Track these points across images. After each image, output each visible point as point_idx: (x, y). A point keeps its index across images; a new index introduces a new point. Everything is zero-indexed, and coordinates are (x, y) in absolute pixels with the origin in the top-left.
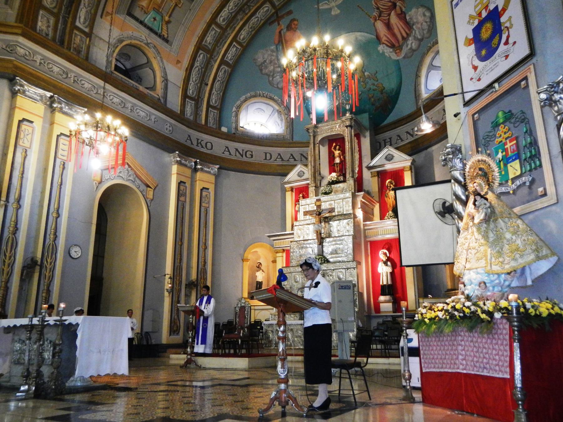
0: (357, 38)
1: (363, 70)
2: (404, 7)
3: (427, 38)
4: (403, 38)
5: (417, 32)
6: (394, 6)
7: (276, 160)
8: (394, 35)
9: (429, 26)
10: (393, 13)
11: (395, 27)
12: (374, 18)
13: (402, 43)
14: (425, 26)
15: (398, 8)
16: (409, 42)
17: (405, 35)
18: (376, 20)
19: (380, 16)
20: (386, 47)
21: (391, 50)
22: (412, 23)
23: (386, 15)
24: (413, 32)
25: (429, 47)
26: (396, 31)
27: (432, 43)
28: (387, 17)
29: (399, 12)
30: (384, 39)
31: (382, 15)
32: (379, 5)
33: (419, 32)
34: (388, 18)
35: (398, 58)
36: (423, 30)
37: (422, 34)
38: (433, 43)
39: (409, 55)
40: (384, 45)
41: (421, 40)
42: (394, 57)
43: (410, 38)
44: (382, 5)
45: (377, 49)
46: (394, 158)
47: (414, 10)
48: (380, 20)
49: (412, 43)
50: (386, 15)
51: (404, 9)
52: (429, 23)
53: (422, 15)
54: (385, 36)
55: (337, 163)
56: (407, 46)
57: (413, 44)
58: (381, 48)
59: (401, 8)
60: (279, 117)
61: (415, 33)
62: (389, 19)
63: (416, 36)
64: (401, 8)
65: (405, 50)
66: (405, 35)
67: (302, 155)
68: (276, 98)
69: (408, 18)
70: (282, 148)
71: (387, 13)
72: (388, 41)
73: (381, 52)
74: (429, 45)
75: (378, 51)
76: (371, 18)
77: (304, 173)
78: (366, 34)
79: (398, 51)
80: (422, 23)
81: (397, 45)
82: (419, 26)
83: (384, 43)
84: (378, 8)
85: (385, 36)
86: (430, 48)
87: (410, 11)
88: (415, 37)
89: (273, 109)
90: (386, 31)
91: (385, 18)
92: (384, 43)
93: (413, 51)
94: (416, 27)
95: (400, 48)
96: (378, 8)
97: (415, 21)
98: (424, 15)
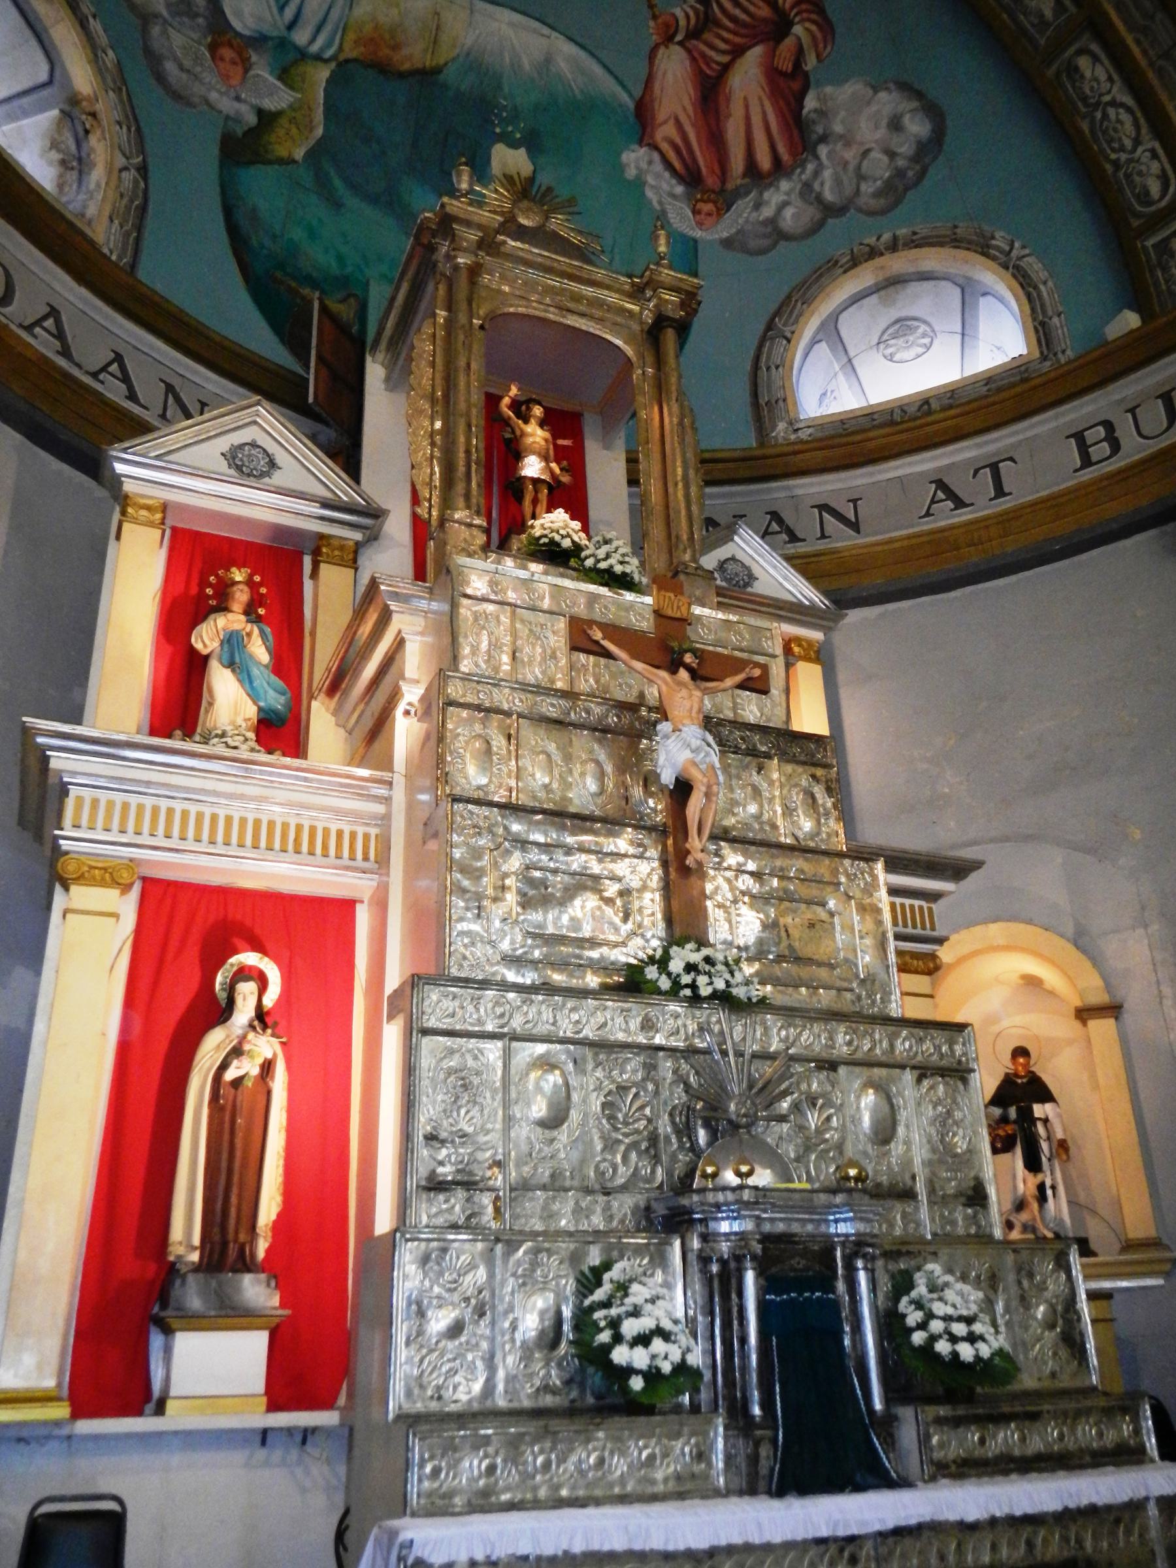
0: (548, 60)
2: (818, 56)
3: (871, 213)
4: (751, 167)
5: (827, 174)
6: (779, 28)
7: (29, 328)
8: (716, 140)
9: (900, 173)
10: (756, 53)
11: (737, 110)
12: (667, 25)
13: (737, 188)
14: (879, 167)
15: (789, 42)
16: (772, 198)
17: (764, 161)
18: (668, 39)
19: (694, 34)
20: (658, 166)
21: (679, 189)
22: (820, 129)
24: (810, 167)
25: (867, 249)
27: (887, 237)
28: (724, 52)
29: (788, 66)
30: (665, 132)
31: (707, 36)
33: (838, 182)
34: (725, 59)
35: (698, 234)
36: (861, 177)
37: (849, 191)
38: (895, 238)
39: (753, 244)
40: (656, 156)
41: (830, 211)
42: (681, 218)
43: (785, 185)
45: (619, 155)
46: (756, 584)
47: (852, 89)
48: (689, 51)
49: (785, 204)
50: (723, 46)
51: (811, 63)
52: (901, 163)
53: (884, 122)
54: (678, 122)
55: (536, 481)
56: (757, 206)
57: (789, 212)
58: (635, 158)
59: (800, 52)
60: (54, 145)
61: (816, 173)
62: (726, 68)
63: (816, 186)
64: (800, 52)
65: (742, 215)
66: (764, 161)
67: (170, 388)
68: (95, 25)
69: (810, 103)
70: (84, 292)
71: (738, 40)
73: (631, 173)
74: (872, 240)
75: (622, 168)
76: (655, 17)
77: (272, 464)
78: (598, 70)
80: (866, 152)
81: (711, 181)
82: (850, 155)
83: (656, 148)
85: (678, 122)
86: (873, 253)
87: (840, 82)
88: (807, 186)
89: (43, 76)
90: (690, 108)
91: (712, 53)
92: (656, 148)
93: (776, 234)
94: (830, 154)
95: (724, 200)
97: (838, 128)
98: (895, 125)
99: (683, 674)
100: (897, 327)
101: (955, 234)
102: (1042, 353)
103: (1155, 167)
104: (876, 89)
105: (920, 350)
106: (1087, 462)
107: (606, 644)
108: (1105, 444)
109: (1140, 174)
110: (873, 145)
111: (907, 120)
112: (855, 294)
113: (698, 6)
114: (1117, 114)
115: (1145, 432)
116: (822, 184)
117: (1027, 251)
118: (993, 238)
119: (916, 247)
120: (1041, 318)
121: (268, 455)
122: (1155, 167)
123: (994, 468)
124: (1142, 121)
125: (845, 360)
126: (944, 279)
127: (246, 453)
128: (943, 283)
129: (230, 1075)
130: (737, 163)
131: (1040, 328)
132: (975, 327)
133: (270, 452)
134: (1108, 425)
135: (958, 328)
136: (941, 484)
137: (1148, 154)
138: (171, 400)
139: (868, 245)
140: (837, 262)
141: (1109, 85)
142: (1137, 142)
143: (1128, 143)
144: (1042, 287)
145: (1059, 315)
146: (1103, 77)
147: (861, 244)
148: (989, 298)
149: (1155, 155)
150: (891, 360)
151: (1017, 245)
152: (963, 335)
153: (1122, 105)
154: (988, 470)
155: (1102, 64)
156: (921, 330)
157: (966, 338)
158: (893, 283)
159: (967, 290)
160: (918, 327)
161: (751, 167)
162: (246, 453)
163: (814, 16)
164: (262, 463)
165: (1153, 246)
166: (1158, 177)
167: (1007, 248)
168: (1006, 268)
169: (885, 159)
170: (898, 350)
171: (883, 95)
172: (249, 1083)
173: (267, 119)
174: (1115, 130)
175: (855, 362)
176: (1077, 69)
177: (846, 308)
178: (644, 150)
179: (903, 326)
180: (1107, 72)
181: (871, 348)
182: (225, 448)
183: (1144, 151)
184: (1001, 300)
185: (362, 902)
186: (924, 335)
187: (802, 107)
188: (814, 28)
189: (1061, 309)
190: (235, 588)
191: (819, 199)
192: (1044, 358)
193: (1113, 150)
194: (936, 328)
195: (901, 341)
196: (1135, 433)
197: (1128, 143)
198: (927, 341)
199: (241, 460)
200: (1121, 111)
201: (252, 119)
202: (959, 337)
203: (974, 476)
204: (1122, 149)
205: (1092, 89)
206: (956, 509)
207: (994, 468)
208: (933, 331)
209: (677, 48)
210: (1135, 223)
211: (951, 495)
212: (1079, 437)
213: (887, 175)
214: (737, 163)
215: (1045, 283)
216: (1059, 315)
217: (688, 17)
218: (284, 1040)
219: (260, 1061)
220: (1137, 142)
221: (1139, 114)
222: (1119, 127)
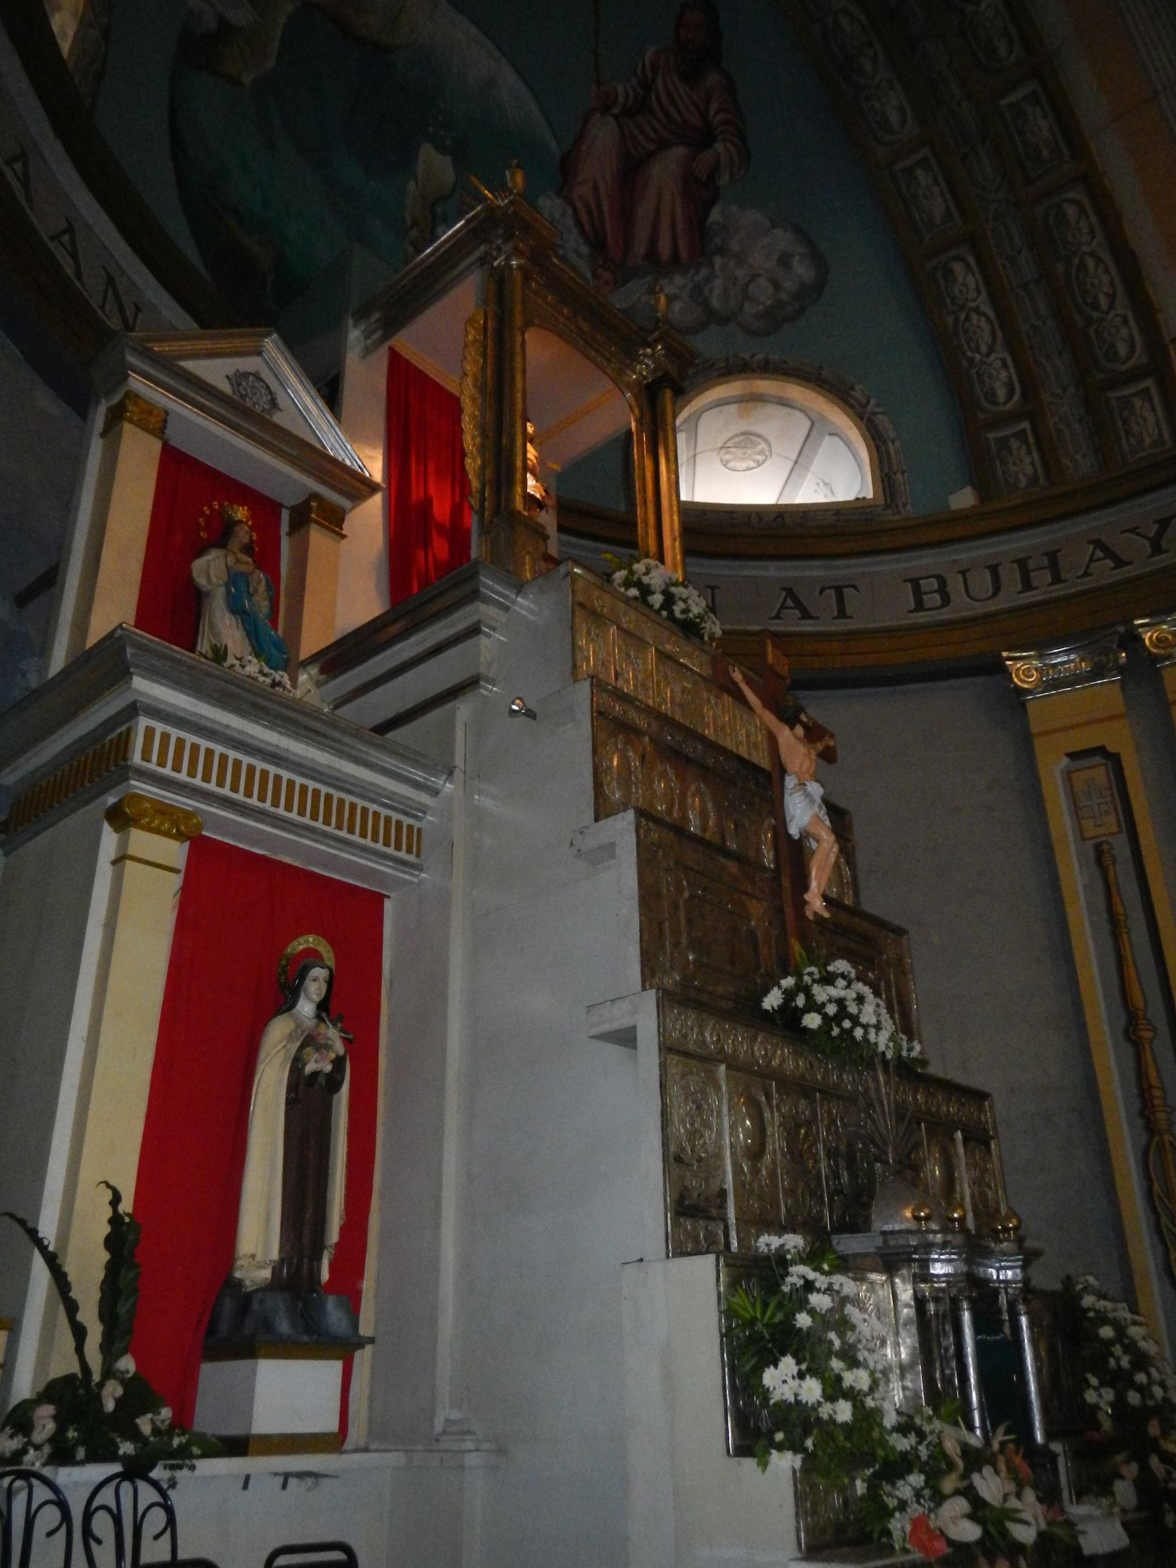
1: (439, 210)
4: (652, 253)
5: (718, 283)
6: (703, 139)
10: (679, 152)
14: (763, 292)
17: (665, 250)
18: (606, 109)
23: (652, 134)
24: (704, 272)
26: (644, 211)
27: (760, 357)
32: (659, 81)
34: (651, 147)
40: (570, 211)
43: (679, 280)
44: (669, 94)
48: (621, 127)
50: (652, 134)
51: (724, 179)
52: (784, 297)
53: (776, 256)
54: (596, 188)
61: (709, 279)
63: (706, 293)
66: (665, 250)
69: (715, 215)
72: (589, 212)
74: (747, 356)
79: (607, 275)
80: (755, 277)
83: (571, 203)
84: (647, 85)
85: (596, 188)
88: (698, 288)
91: (640, 137)
96: (647, 85)
97: (735, 247)
98: (784, 261)
99: (799, 730)
100: (743, 437)
101: (820, 374)
102: (886, 501)
103: (1003, 375)
104: (774, 226)
105: (752, 464)
106: (920, 606)
107: (744, 687)
108: (937, 596)
109: (990, 376)
110: (761, 272)
111: (795, 261)
112: (722, 399)
113: (639, 90)
114: (979, 320)
115: (972, 594)
116: (711, 291)
117: (880, 410)
118: (852, 388)
119: (784, 374)
120: (887, 470)
121: (270, 392)
122: (1003, 375)
123: (839, 591)
124: (999, 332)
125: (692, 454)
126: (800, 410)
127: (250, 383)
128: (798, 414)
129: (310, 1068)
130: (640, 247)
131: (886, 479)
132: (811, 460)
133: (273, 390)
134: (942, 581)
135: (794, 457)
136: (790, 593)
137: (999, 362)
138: (110, 295)
139: (743, 359)
140: (713, 364)
141: (975, 295)
142: (991, 350)
143: (984, 349)
144: (890, 444)
145: (903, 473)
146: (972, 285)
147: (736, 356)
148: (836, 440)
149: (1005, 365)
150: (725, 466)
151: (873, 401)
152: (796, 462)
153: (985, 315)
154: (833, 591)
155: (974, 275)
156: (760, 447)
157: (797, 466)
158: (756, 399)
159: (817, 425)
160: (759, 444)
161: (652, 253)
162: (250, 383)
163: (735, 140)
164: (264, 399)
165: (995, 439)
166: (1005, 384)
167: (864, 401)
168: (862, 419)
169: (770, 289)
170: (734, 459)
171: (778, 232)
172: (322, 1080)
173: (226, 29)
174: (975, 333)
175: (698, 458)
176: (951, 271)
177: (713, 407)
178: (558, 201)
179: (747, 439)
180: (977, 283)
181: (714, 450)
182: (231, 372)
183: (996, 359)
184: (848, 445)
185: (388, 897)
186: (761, 452)
187: (707, 215)
188: (732, 149)
189: (904, 468)
190: (237, 528)
191: (706, 303)
192: (887, 507)
193: (970, 349)
194: (773, 450)
195: (739, 452)
196: (964, 594)
197: (984, 349)
198: (760, 458)
199: (245, 389)
200: (983, 319)
201: (213, 26)
202: (790, 464)
203: (821, 593)
204: (978, 350)
205: (961, 292)
206: (802, 618)
207: (839, 591)
208: (771, 451)
209: (612, 120)
210: (982, 416)
211: (799, 605)
212: (915, 582)
213: (769, 303)
214: (640, 247)
215: (893, 442)
216: (903, 473)
217: (627, 95)
218: (351, 1037)
219: (332, 1056)
220: (991, 350)
221: (997, 327)
222: (979, 331)
